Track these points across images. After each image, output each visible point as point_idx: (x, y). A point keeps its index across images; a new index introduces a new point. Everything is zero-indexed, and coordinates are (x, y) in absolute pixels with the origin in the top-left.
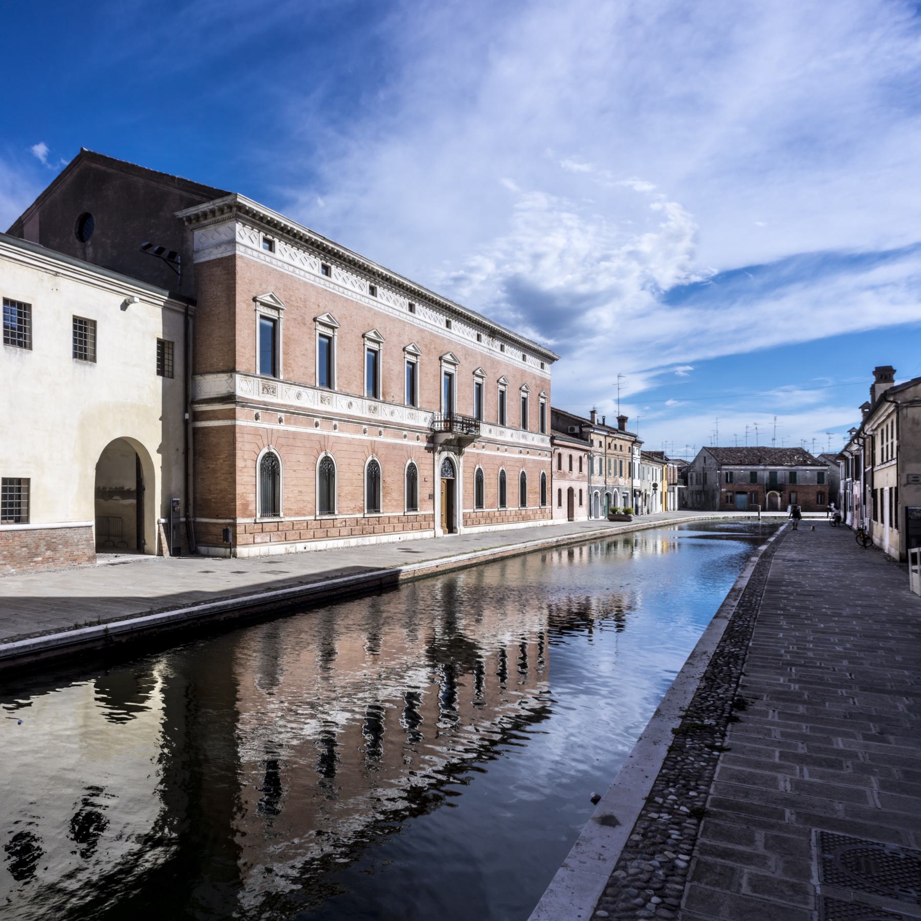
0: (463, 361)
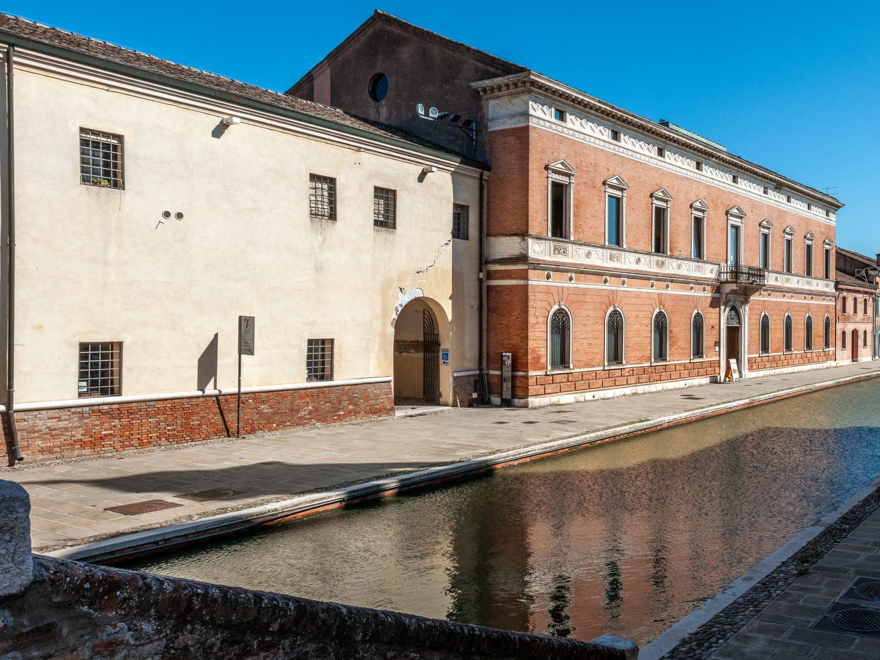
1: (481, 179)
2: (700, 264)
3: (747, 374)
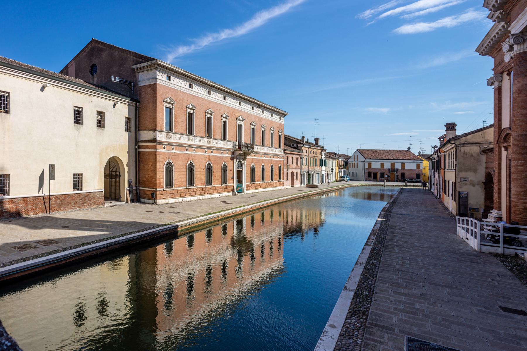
1: (136, 106)
3: (246, 192)
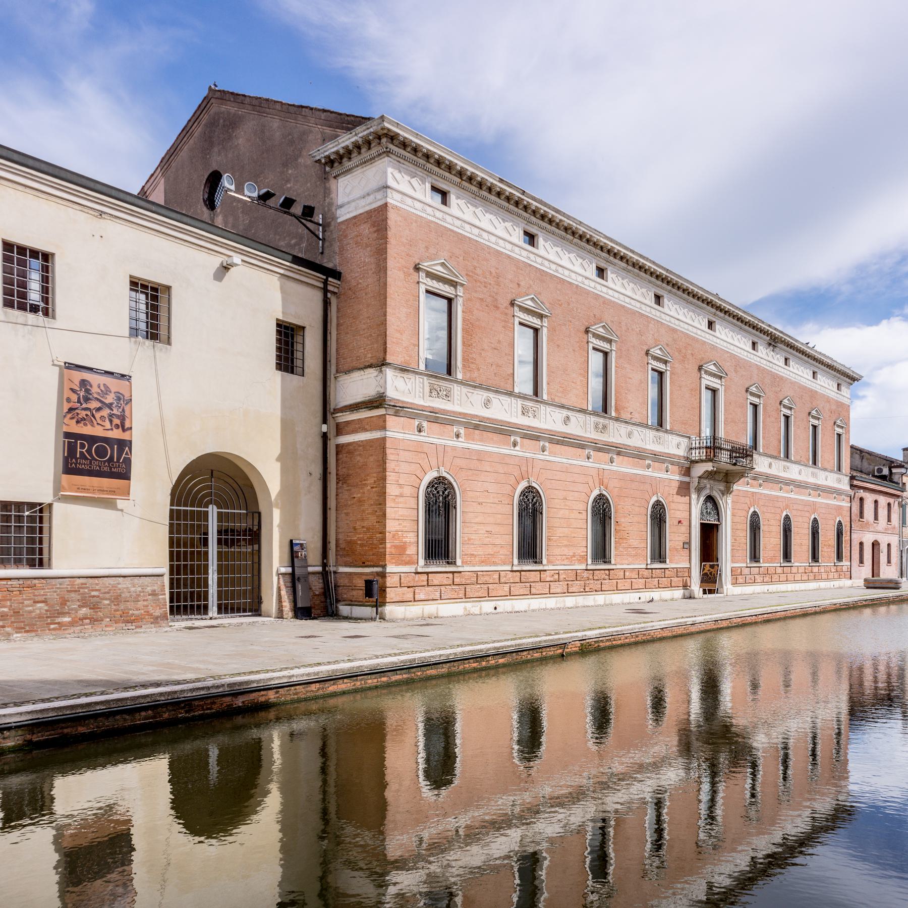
0: (732, 374)
2: (661, 434)
